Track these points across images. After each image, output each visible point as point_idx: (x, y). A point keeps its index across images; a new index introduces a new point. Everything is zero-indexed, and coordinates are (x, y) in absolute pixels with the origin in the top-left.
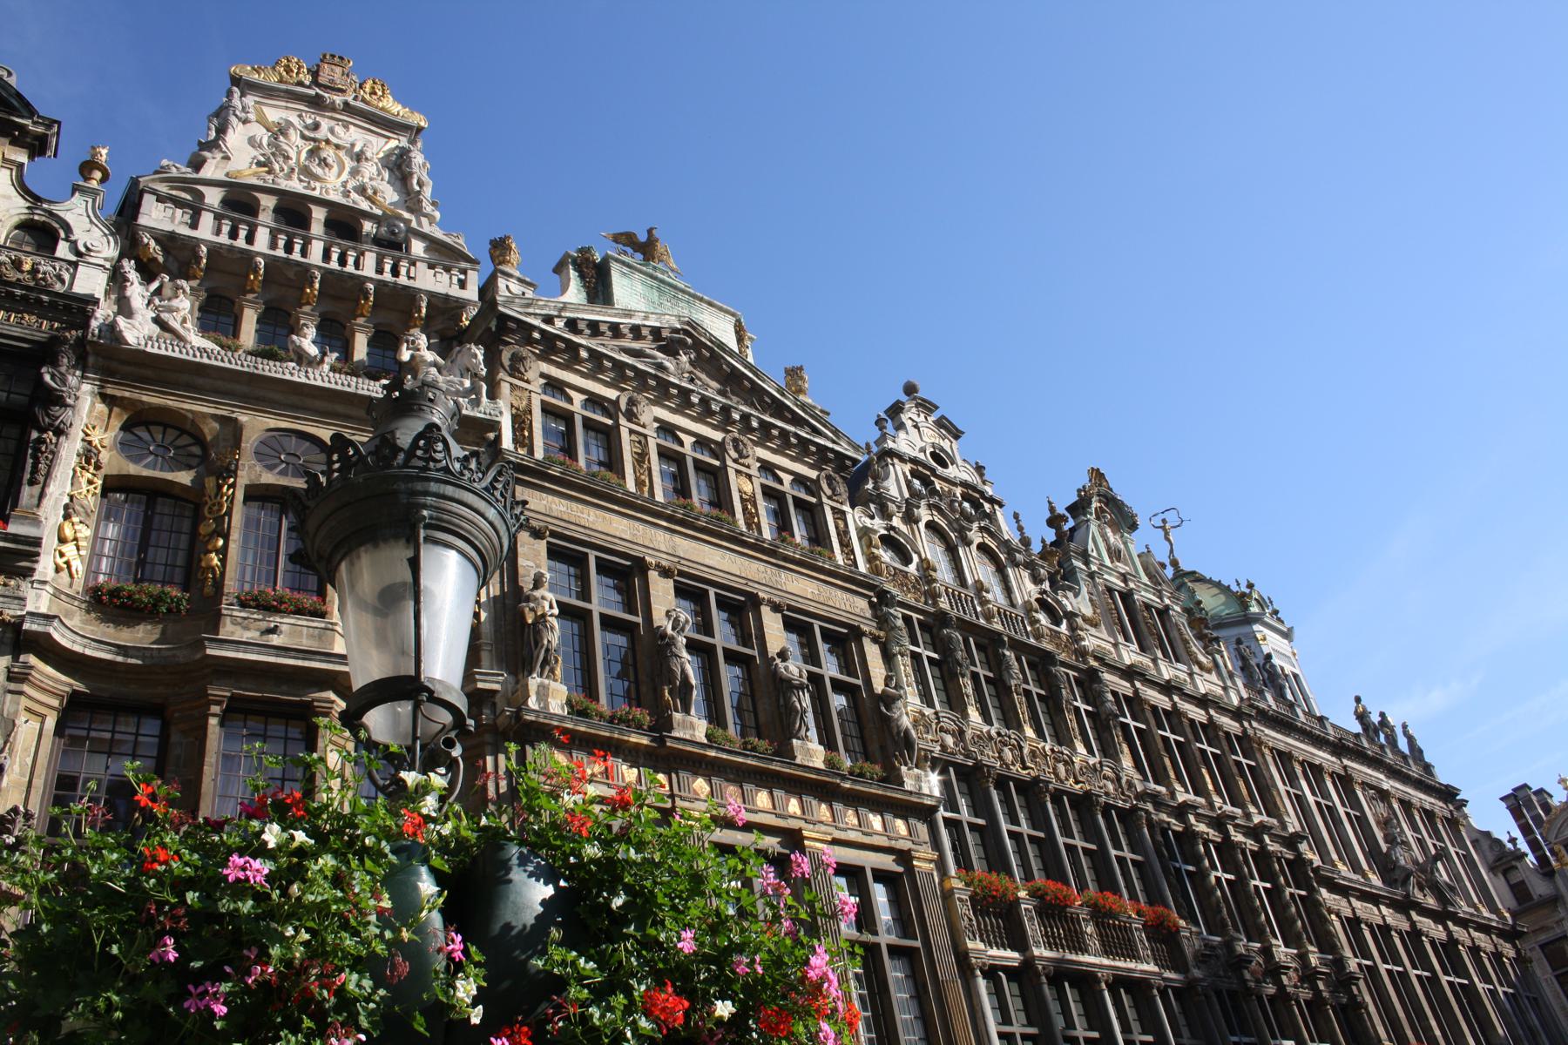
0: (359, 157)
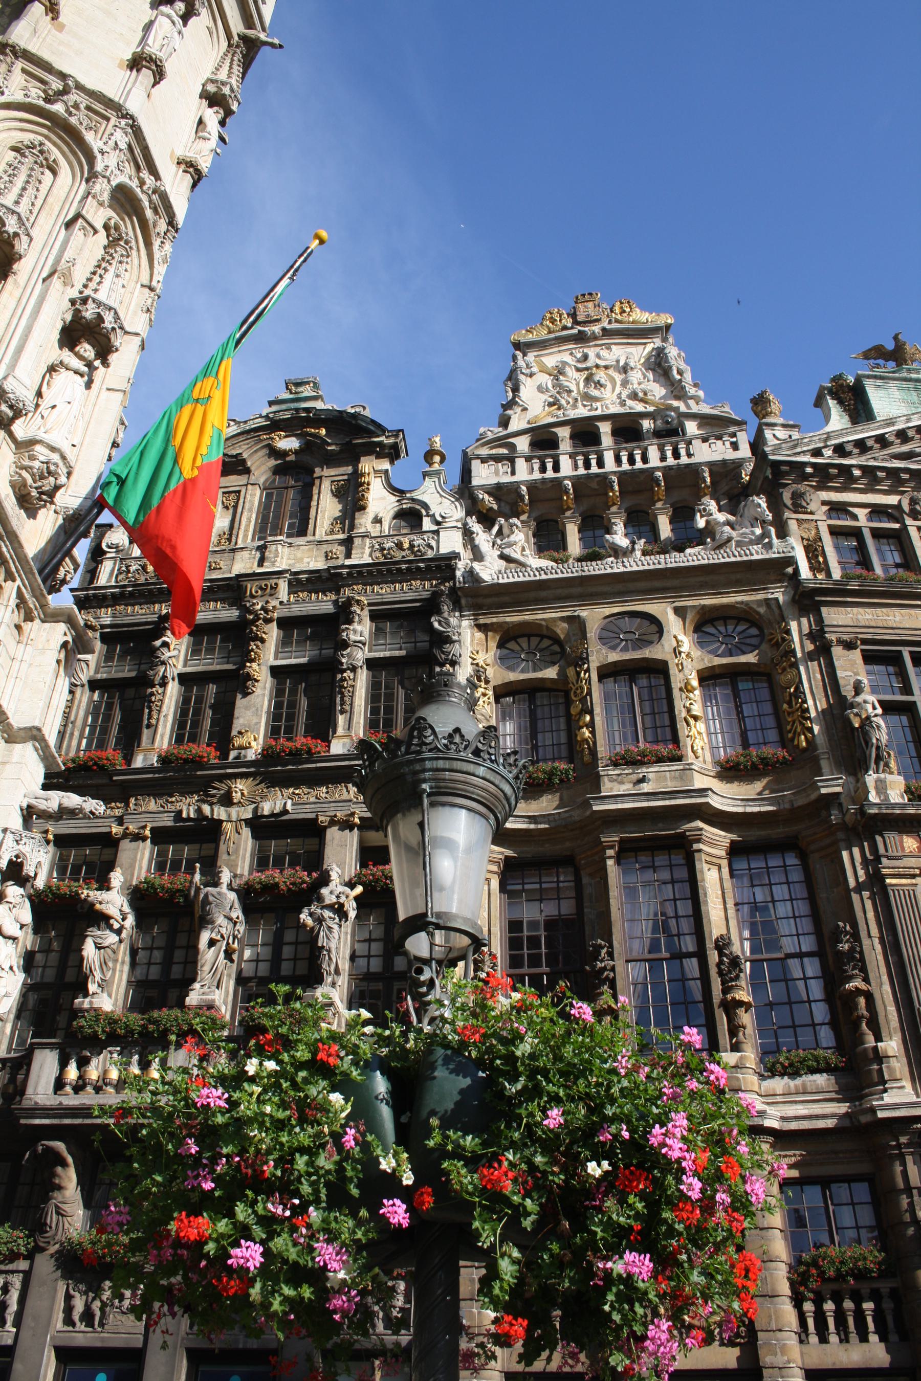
0: (625, 369)
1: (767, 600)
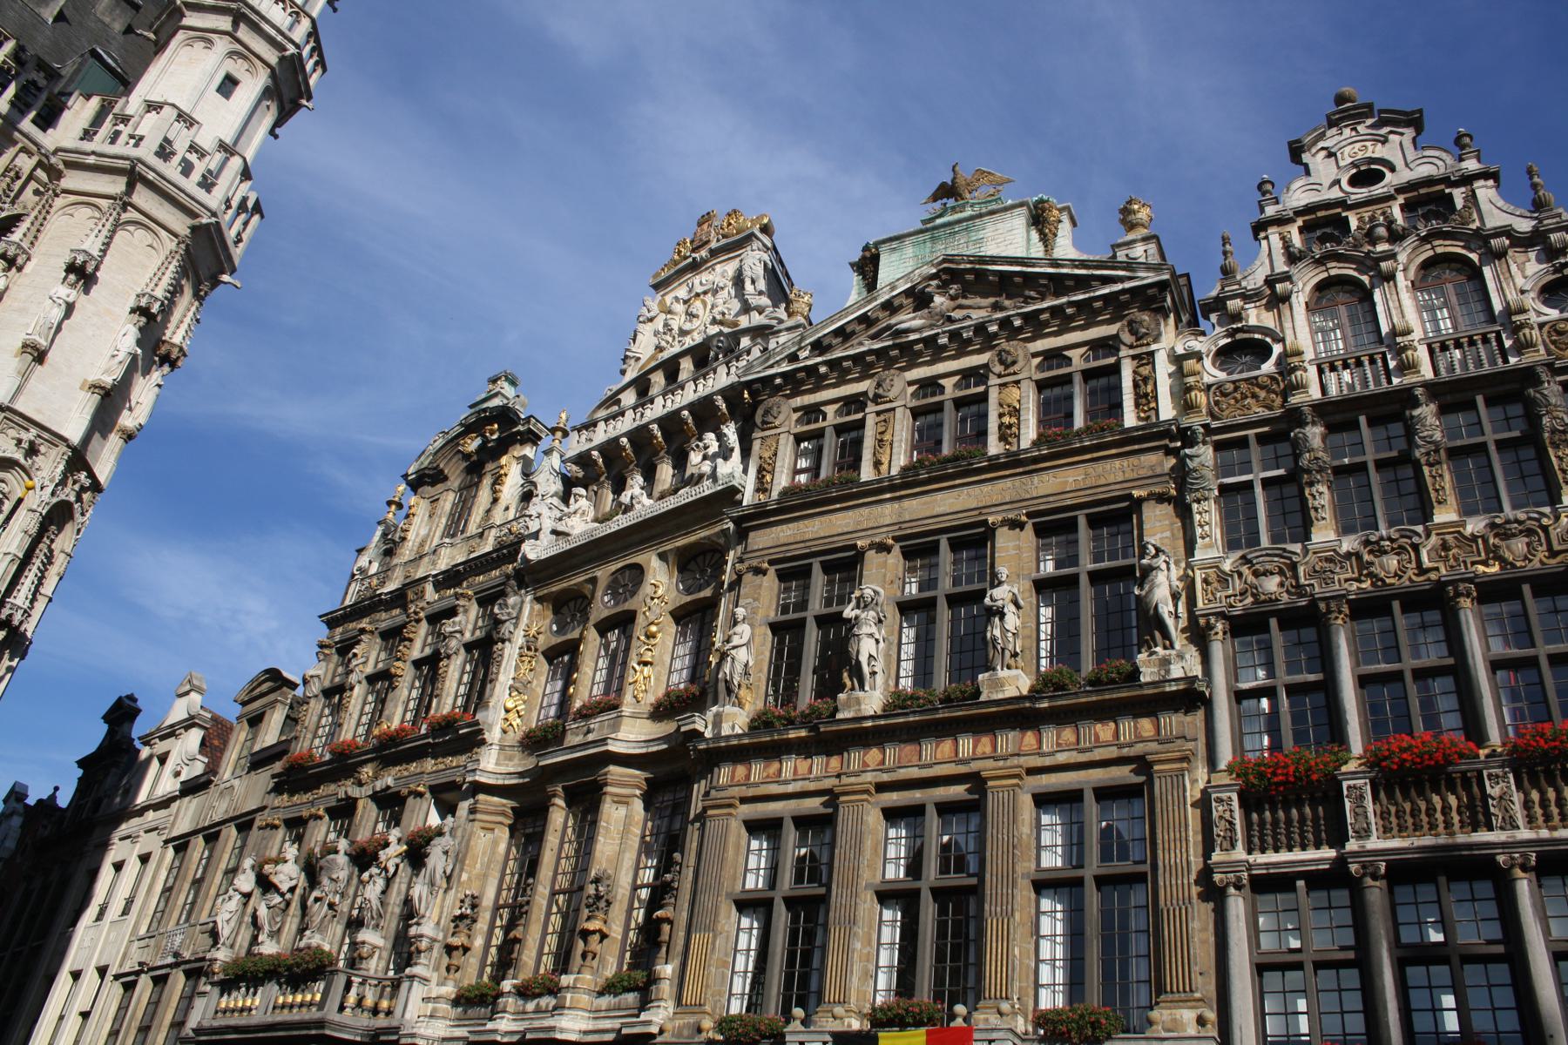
0: (715, 292)
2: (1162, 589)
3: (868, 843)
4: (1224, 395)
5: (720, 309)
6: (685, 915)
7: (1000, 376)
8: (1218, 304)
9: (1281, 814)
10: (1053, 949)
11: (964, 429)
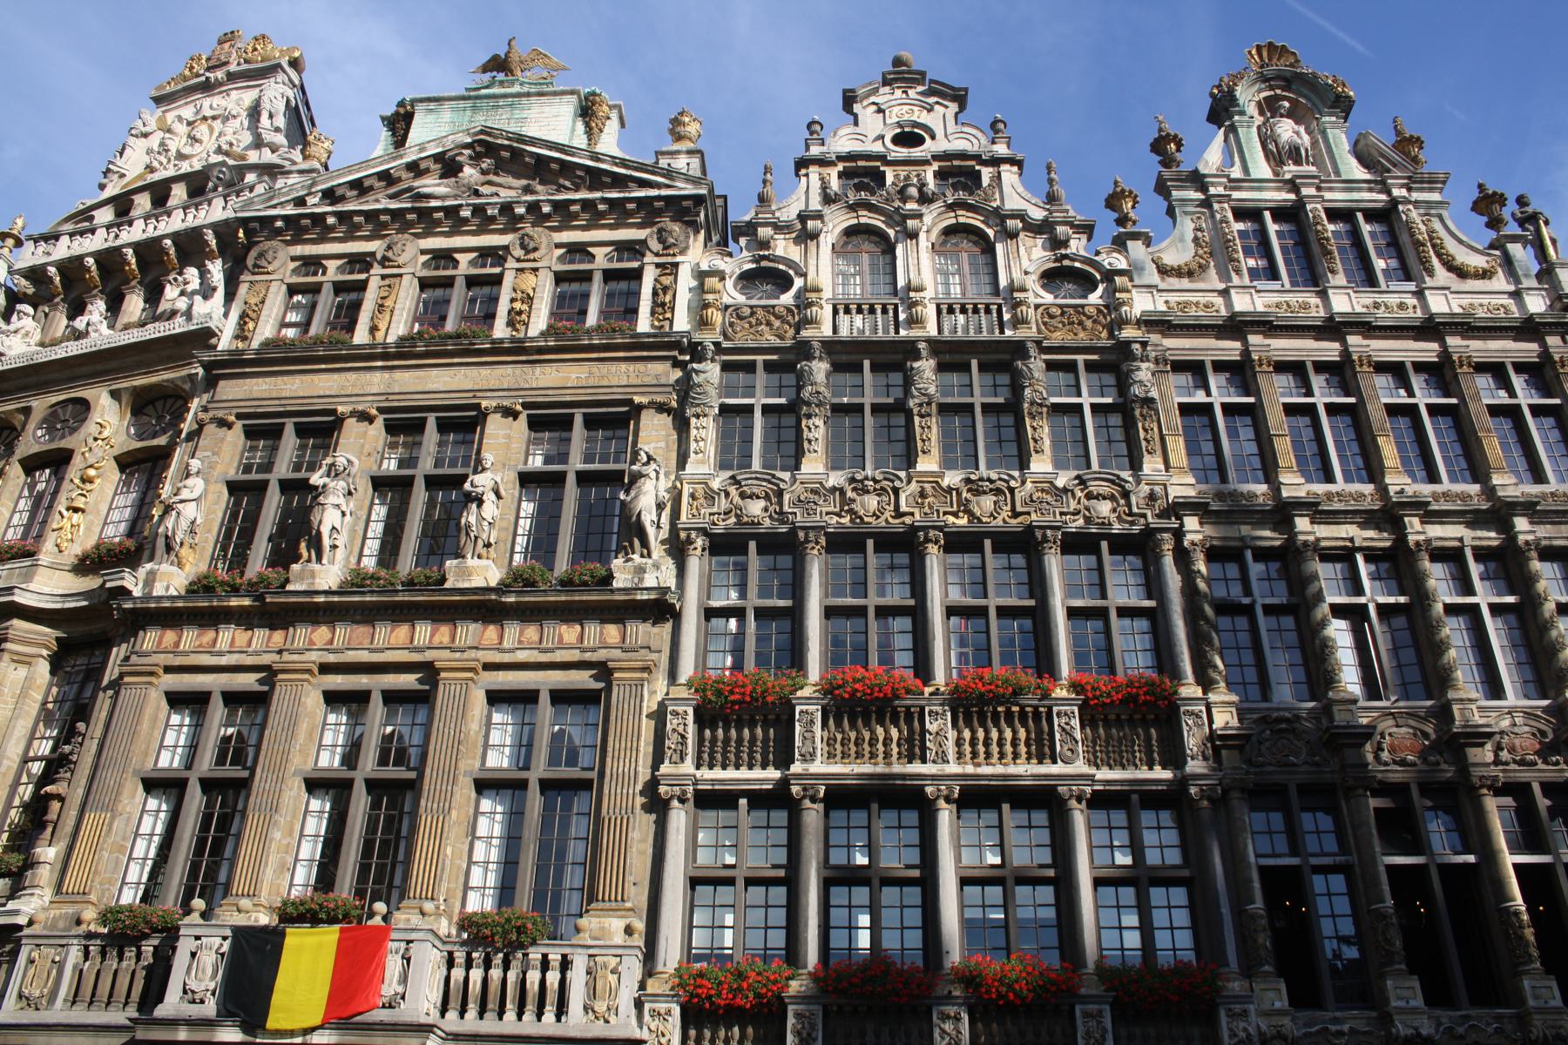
1: (190, 376)
2: (647, 499)
3: (303, 727)
4: (740, 318)
5: (228, 138)
6: (80, 791)
7: (518, 260)
8: (749, 229)
9: (733, 733)
10: (488, 852)
11: (472, 309)
